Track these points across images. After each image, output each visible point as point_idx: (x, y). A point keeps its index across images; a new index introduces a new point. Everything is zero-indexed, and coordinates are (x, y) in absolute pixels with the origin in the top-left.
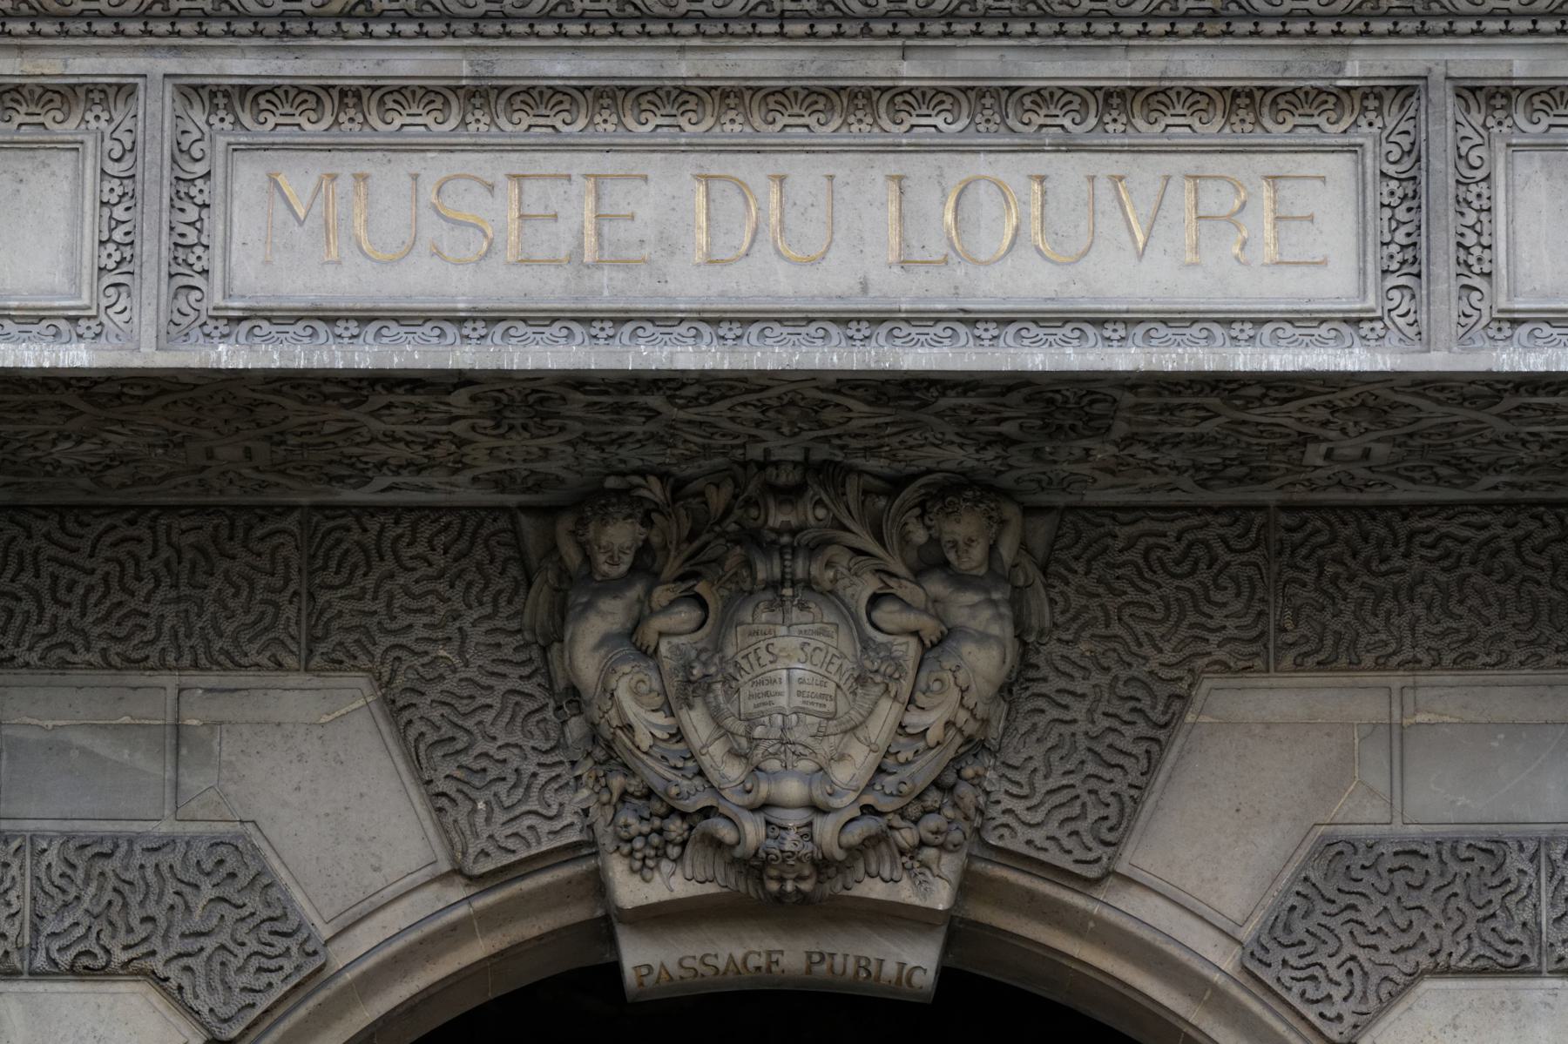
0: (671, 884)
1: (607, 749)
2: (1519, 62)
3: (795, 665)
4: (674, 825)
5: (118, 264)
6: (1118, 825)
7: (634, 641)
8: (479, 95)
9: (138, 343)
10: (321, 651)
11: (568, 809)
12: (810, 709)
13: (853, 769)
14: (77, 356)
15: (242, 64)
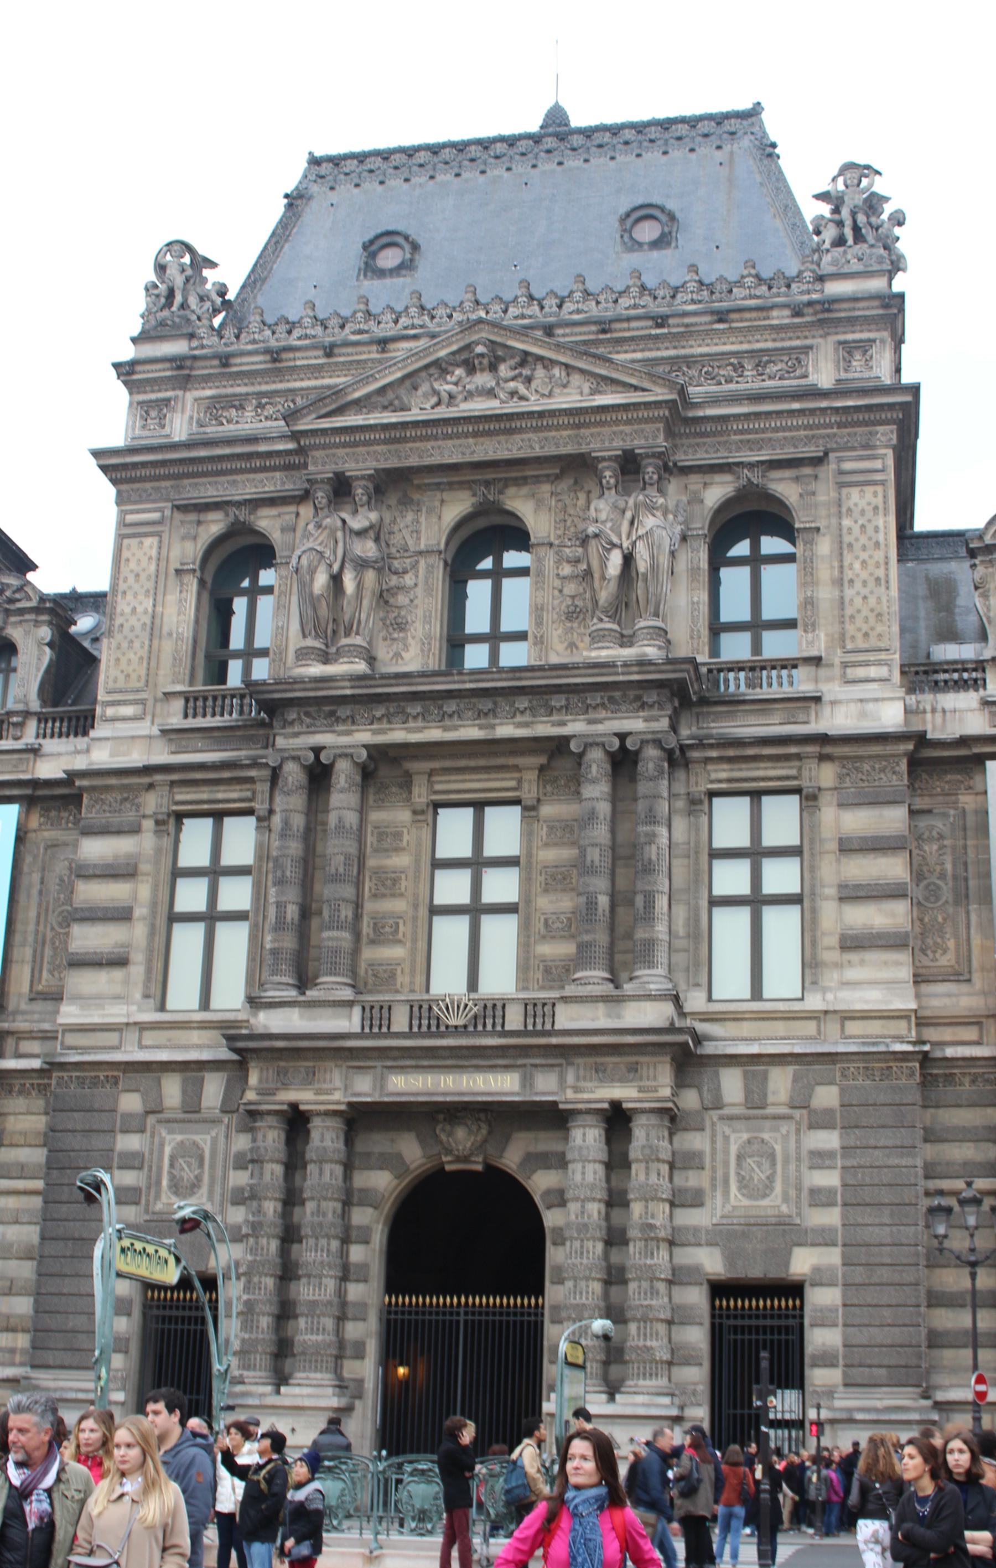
0: (449, 1158)
1: (441, 1142)
2: (537, 1061)
3: (461, 1133)
4: (449, 1151)
5: (374, 1088)
6: (503, 1150)
7: (443, 1130)
8: (417, 1067)
9: (376, 1098)
10: (409, 1129)
11: (436, 1149)
12: (462, 1138)
13: (469, 1145)
14: (369, 1099)
15: (389, 1063)
